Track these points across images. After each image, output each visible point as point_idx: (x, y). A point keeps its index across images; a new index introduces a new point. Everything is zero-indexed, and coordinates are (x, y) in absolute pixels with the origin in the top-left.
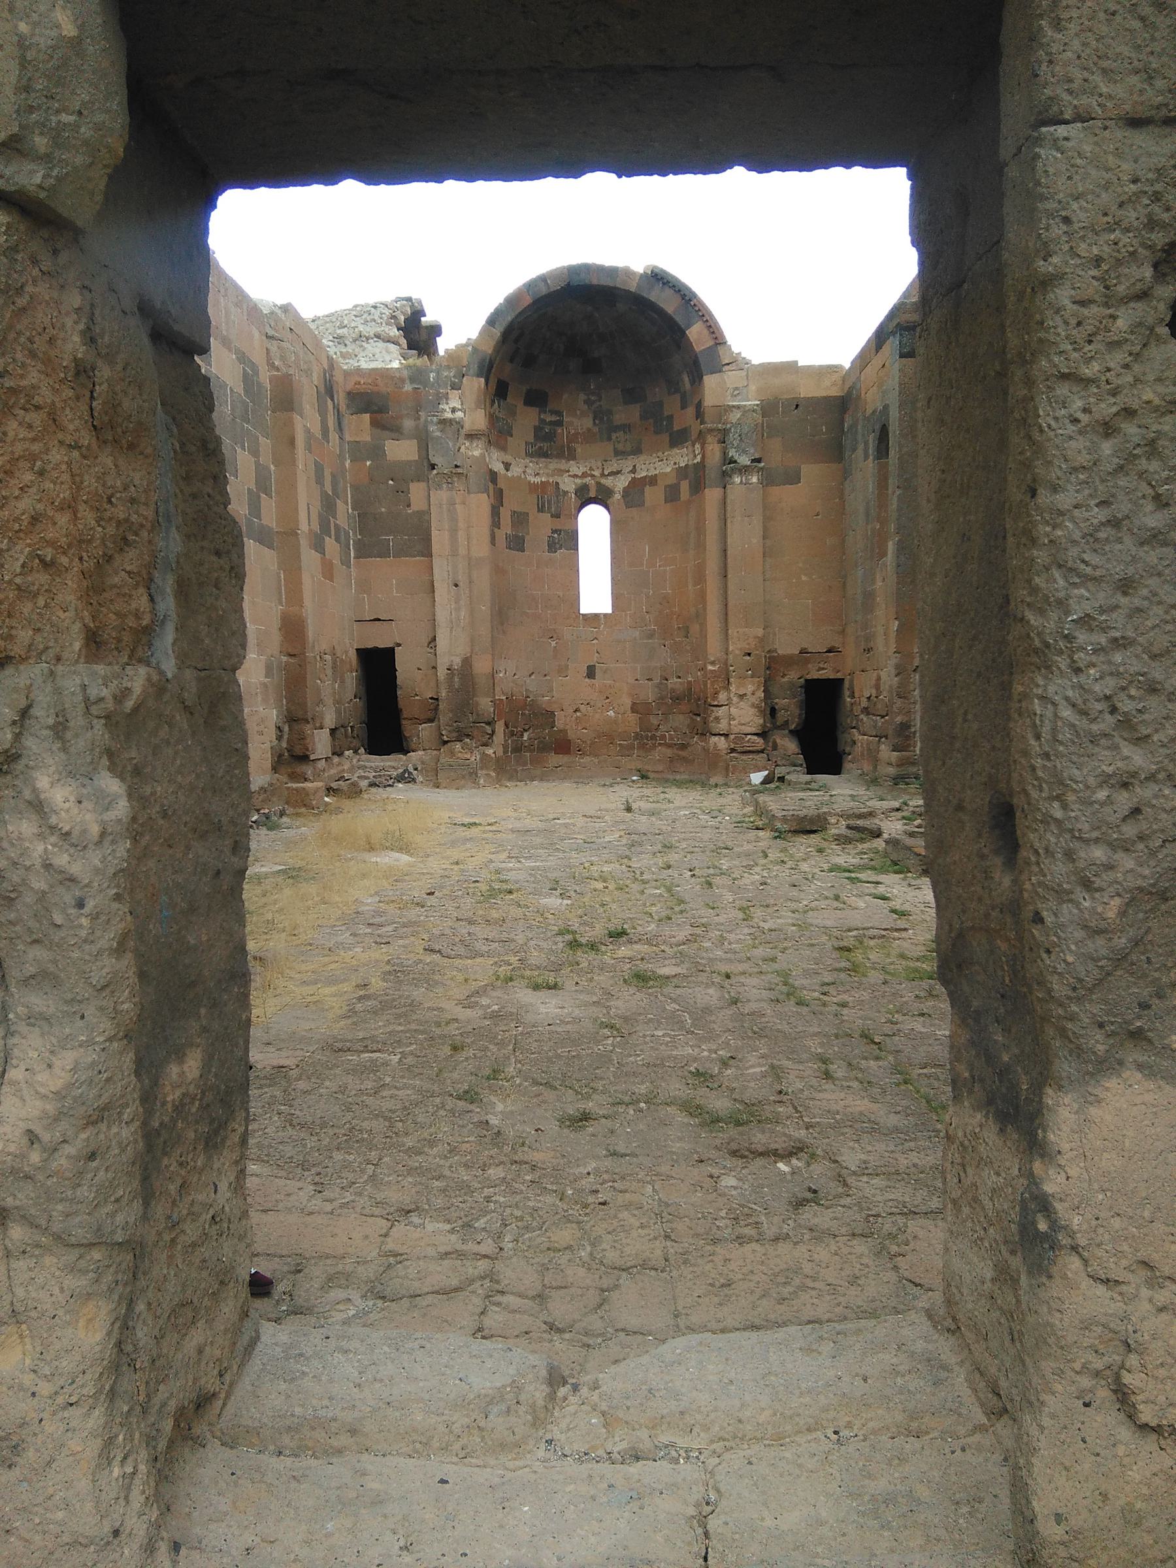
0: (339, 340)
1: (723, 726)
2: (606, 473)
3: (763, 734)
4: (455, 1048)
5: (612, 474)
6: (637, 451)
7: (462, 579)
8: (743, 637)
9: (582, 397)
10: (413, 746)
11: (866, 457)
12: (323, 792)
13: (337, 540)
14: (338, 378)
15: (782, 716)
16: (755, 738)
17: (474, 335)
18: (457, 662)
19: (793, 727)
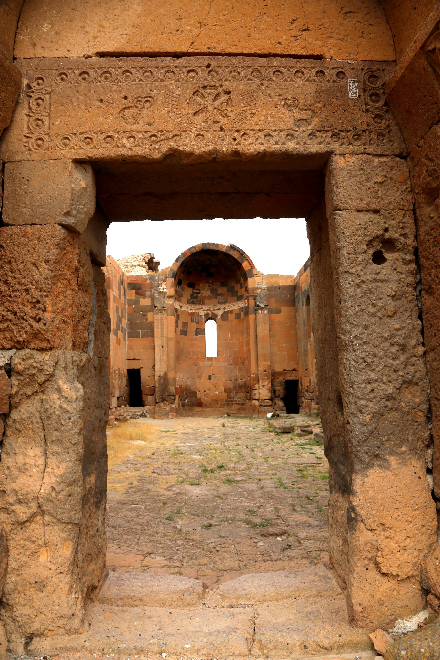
0: (126, 266)
1: (257, 397)
3: (271, 399)
4: (164, 504)
5: (217, 310)
6: (226, 302)
7: (165, 345)
8: (263, 365)
9: (207, 284)
10: (146, 404)
11: (303, 305)
12: (114, 420)
13: (122, 332)
14: (125, 278)
15: (278, 393)
17: (171, 265)
18: (162, 374)
19: (281, 397)
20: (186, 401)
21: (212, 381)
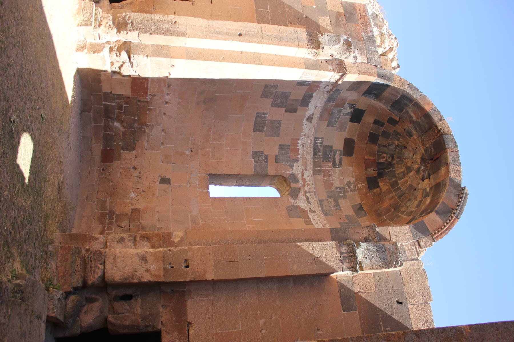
2: (307, 194)
5: (307, 198)
9: (352, 180)
15: (122, 306)
16: (100, 274)
19: (111, 318)
20: (117, 124)
21: (158, 186)
